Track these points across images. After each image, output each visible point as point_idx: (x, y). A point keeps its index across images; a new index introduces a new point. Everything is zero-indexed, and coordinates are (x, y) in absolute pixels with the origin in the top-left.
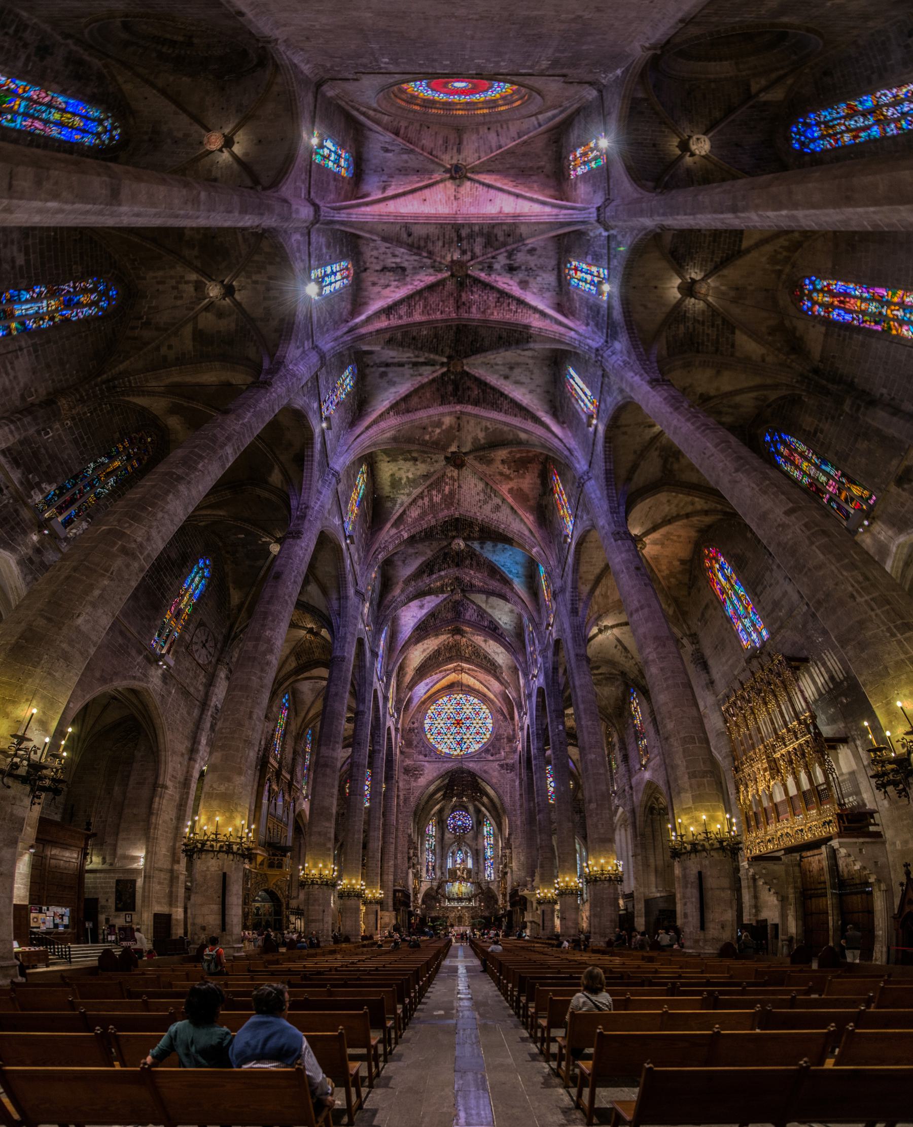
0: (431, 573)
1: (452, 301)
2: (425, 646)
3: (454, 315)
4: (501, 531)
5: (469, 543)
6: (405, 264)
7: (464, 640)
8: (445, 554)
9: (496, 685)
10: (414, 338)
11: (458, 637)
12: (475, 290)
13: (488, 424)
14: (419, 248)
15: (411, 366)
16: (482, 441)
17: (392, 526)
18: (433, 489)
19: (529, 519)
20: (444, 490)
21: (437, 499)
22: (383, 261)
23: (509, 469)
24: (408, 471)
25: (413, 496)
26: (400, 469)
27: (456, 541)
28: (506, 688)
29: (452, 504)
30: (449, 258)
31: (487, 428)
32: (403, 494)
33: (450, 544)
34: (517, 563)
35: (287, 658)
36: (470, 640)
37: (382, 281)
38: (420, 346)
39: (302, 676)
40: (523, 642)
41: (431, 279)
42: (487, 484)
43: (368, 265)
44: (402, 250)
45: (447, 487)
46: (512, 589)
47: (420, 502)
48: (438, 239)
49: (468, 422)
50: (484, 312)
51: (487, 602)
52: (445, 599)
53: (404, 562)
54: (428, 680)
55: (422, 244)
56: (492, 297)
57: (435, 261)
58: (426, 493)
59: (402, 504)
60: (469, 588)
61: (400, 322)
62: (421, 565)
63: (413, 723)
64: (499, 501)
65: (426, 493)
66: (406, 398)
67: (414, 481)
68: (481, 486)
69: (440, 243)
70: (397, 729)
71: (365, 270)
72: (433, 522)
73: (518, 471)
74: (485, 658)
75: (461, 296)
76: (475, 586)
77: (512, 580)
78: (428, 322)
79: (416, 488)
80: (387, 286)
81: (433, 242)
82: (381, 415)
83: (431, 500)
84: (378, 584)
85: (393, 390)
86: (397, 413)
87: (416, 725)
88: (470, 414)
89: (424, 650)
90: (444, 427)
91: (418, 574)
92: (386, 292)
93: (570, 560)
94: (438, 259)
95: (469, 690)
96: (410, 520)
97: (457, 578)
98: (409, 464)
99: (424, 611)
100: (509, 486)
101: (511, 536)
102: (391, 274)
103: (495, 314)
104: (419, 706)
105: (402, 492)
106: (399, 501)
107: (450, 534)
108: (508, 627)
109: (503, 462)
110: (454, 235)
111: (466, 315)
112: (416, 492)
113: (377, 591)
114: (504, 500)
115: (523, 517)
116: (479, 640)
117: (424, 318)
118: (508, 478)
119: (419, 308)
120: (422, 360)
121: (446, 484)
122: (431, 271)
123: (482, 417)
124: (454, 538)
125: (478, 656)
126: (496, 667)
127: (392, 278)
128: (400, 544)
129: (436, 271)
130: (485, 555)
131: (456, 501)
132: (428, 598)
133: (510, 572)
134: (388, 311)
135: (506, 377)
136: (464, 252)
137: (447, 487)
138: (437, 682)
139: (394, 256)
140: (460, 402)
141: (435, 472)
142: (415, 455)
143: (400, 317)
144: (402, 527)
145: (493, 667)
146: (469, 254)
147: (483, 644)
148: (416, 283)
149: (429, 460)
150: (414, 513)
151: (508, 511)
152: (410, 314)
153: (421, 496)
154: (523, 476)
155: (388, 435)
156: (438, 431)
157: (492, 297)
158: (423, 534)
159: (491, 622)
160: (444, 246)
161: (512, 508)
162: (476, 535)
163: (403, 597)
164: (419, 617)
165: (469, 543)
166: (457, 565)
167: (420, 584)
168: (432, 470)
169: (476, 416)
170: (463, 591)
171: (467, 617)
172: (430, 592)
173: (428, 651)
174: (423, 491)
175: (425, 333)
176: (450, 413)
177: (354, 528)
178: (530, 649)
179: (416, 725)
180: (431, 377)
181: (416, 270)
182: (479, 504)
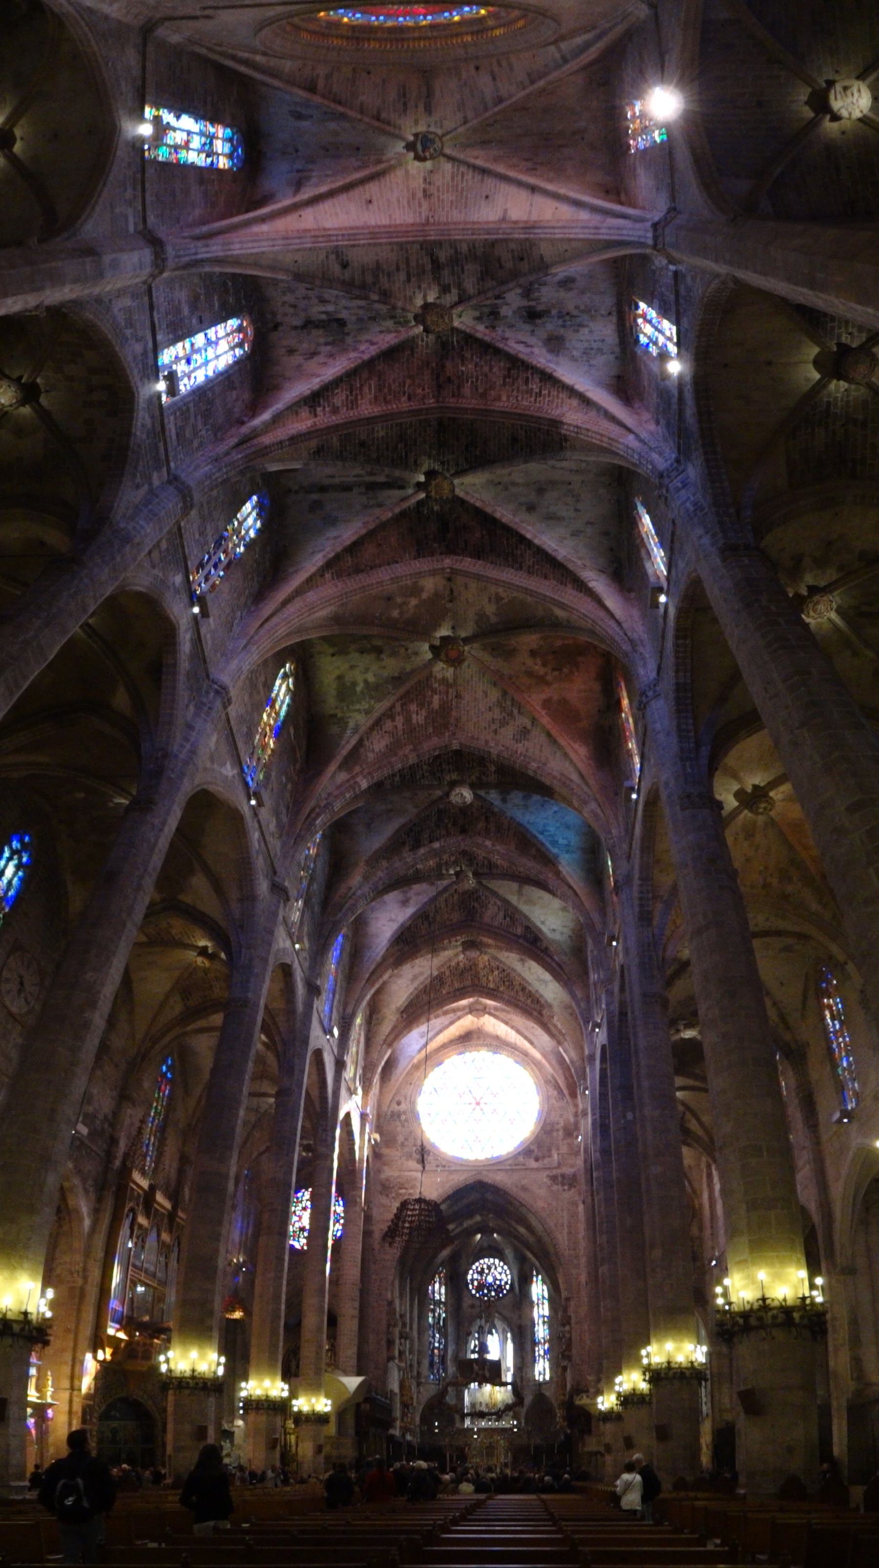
0: (417, 845)
1: (427, 376)
2: (417, 970)
3: (431, 402)
4: (531, 773)
5: (482, 793)
6: (344, 315)
7: (486, 958)
8: (440, 812)
9: (545, 1039)
10: (362, 444)
11: (473, 954)
12: (468, 355)
13: (501, 590)
14: (363, 286)
15: (363, 490)
16: (494, 619)
17: (340, 768)
18: (412, 701)
19: (580, 752)
22: (305, 310)
23: (544, 665)
24: (367, 670)
25: (376, 715)
26: (352, 667)
27: (457, 790)
28: (559, 1043)
29: (446, 726)
30: (419, 302)
31: (499, 599)
32: (359, 711)
33: (447, 795)
34: (568, 827)
35: (167, 997)
36: (496, 959)
37: (305, 345)
38: (374, 456)
39: (189, 1028)
40: (583, 963)
41: (388, 340)
42: (505, 693)
43: (279, 318)
44: (335, 292)
45: (436, 698)
46: (558, 873)
48: (398, 269)
49: (466, 587)
50: (484, 395)
51: (520, 893)
52: (446, 889)
53: (368, 826)
54: (423, 1028)
55: (369, 279)
56: (498, 369)
57: (394, 308)
58: (398, 708)
59: (356, 730)
60: (486, 870)
61: (335, 419)
62: (398, 831)
63: (399, 1103)
64: (527, 723)
65: (398, 708)
66: (353, 548)
67: (377, 687)
68: (494, 695)
69: (402, 276)
70: (363, 1117)
71: (276, 327)
72: (412, 760)
73: (559, 669)
74: (523, 989)
75: (443, 367)
76: (497, 866)
77: (557, 857)
78: (384, 418)
79: (379, 700)
80: (314, 354)
81: (389, 275)
82: (309, 580)
83: (408, 720)
84: (321, 869)
85: (332, 533)
86: (339, 575)
87: (403, 1107)
88: (467, 574)
89: (415, 977)
90: (425, 596)
91: (393, 848)
92: (312, 365)
93: (638, 830)
94: (400, 304)
95: (498, 1044)
96: (371, 756)
97: (464, 853)
99: (410, 911)
100: (544, 696)
101: (548, 783)
102: (321, 332)
103: (504, 398)
104: (409, 1074)
105: (357, 707)
106: (351, 724)
107: (448, 778)
108: (557, 937)
109: (533, 653)
111: (452, 402)
112: (381, 707)
113: (321, 877)
114: (534, 721)
115: (569, 750)
116: (511, 959)
117: (376, 410)
118: (542, 680)
119: (369, 392)
120: (382, 479)
121: (434, 691)
122: (389, 323)
123: (488, 580)
124: (453, 784)
125: (511, 985)
126: (542, 1006)
127: (322, 340)
128: (356, 798)
129: (399, 323)
130: (509, 814)
131: (452, 721)
132: (416, 887)
133: (555, 843)
134: (313, 400)
135: (531, 508)
136: (445, 289)
138: (441, 1031)
139: (323, 301)
140: (450, 551)
141: (413, 671)
142: (378, 643)
143: (335, 411)
144: (357, 769)
145: (538, 1007)
146: (454, 291)
147: (518, 966)
148: (362, 347)
149: (402, 650)
150: (379, 744)
151: (543, 738)
152: (352, 404)
153: (389, 714)
155: (323, 613)
156: (414, 602)
157: (498, 369)
158: (397, 779)
159: (527, 928)
160: (409, 281)
161: (549, 735)
162: (493, 778)
163: (366, 889)
165: (482, 793)
166: (463, 831)
167: (397, 864)
168: (408, 668)
169: (478, 577)
170: (476, 874)
171: (487, 919)
172: (417, 878)
173: (422, 979)
174: (393, 706)
175: (382, 433)
176: (433, 573)
177: (267, 777)
178: (593, 977)
179: (403, 1107)
180: (397, 510)
181: (363, 324)
182: (494, 727)
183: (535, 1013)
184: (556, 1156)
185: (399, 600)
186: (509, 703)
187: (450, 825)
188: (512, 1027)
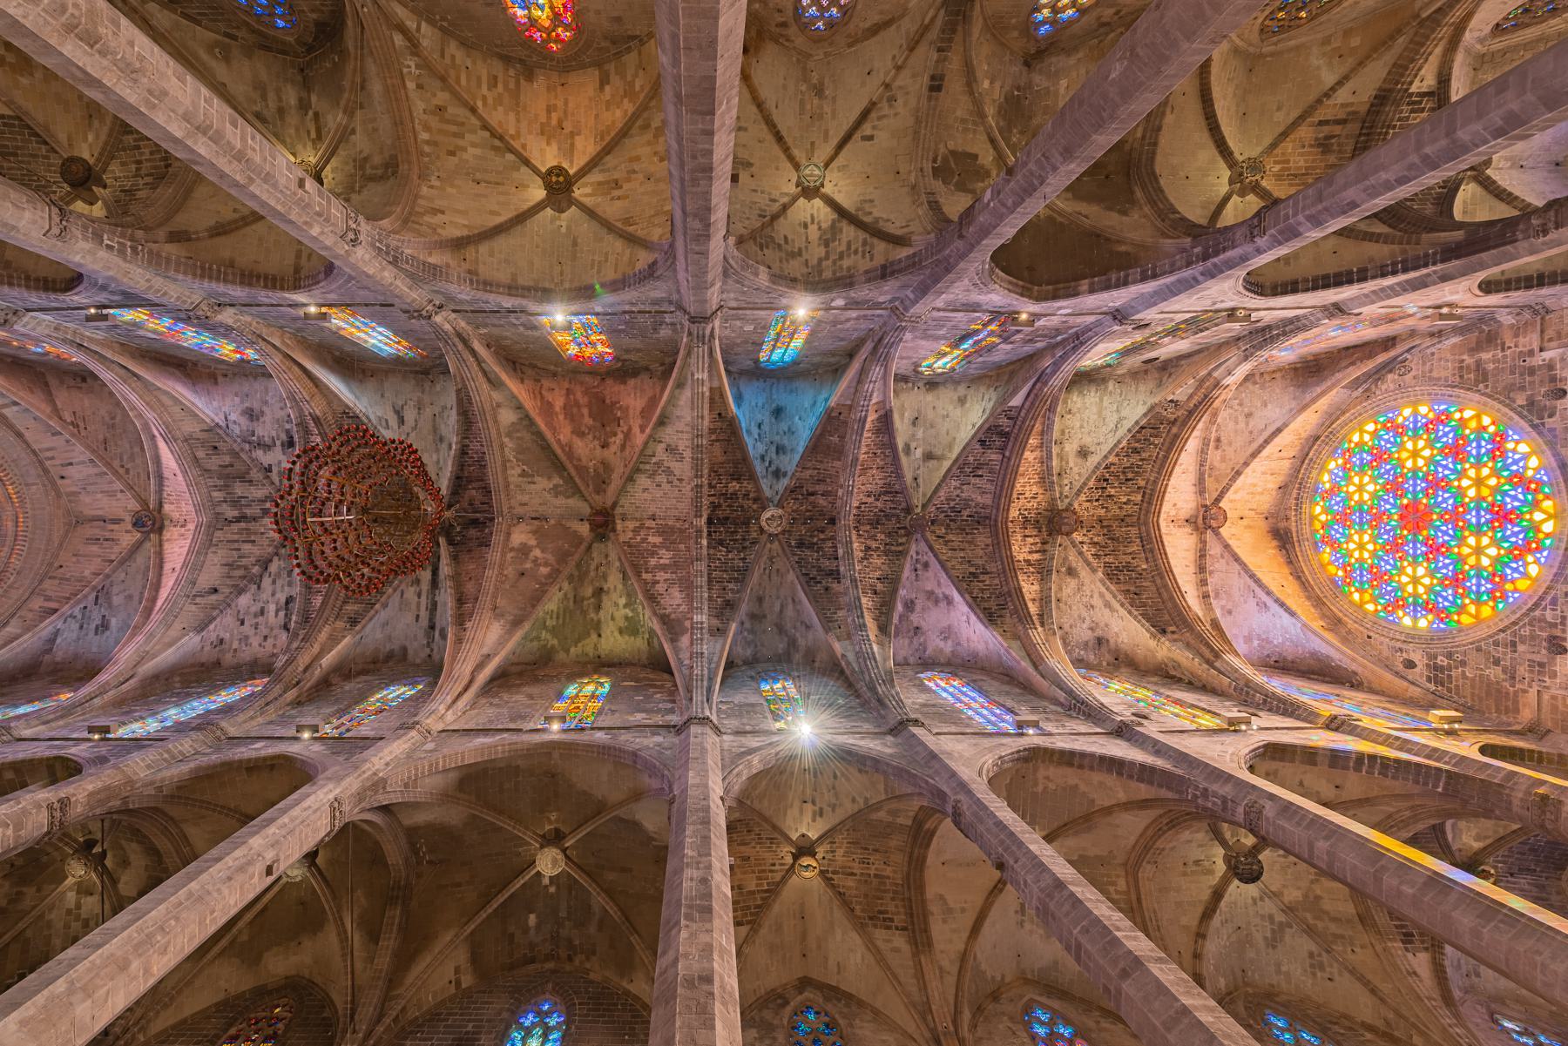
20: (655, 545)
21: (666, 557)
24: (616, 605)
45: (651, 539)
47: (660, 588)
64: (660, 448)
68: (643, 481)
83: (664, 568)
98: (607, 602)
110: (235, 527)
121: (644, 540)
137: (651, 539)
138: (1252, 576)
142: (589, 591)
154: (626, 410)
156: (537, 553)
164: (965, 609)
182: (676, 483)
183: (1175, 430)
184: (1547, 355)
185: (528, 565)
186: (647, 467)
187: (822, 536)
188: (1246, 464)
